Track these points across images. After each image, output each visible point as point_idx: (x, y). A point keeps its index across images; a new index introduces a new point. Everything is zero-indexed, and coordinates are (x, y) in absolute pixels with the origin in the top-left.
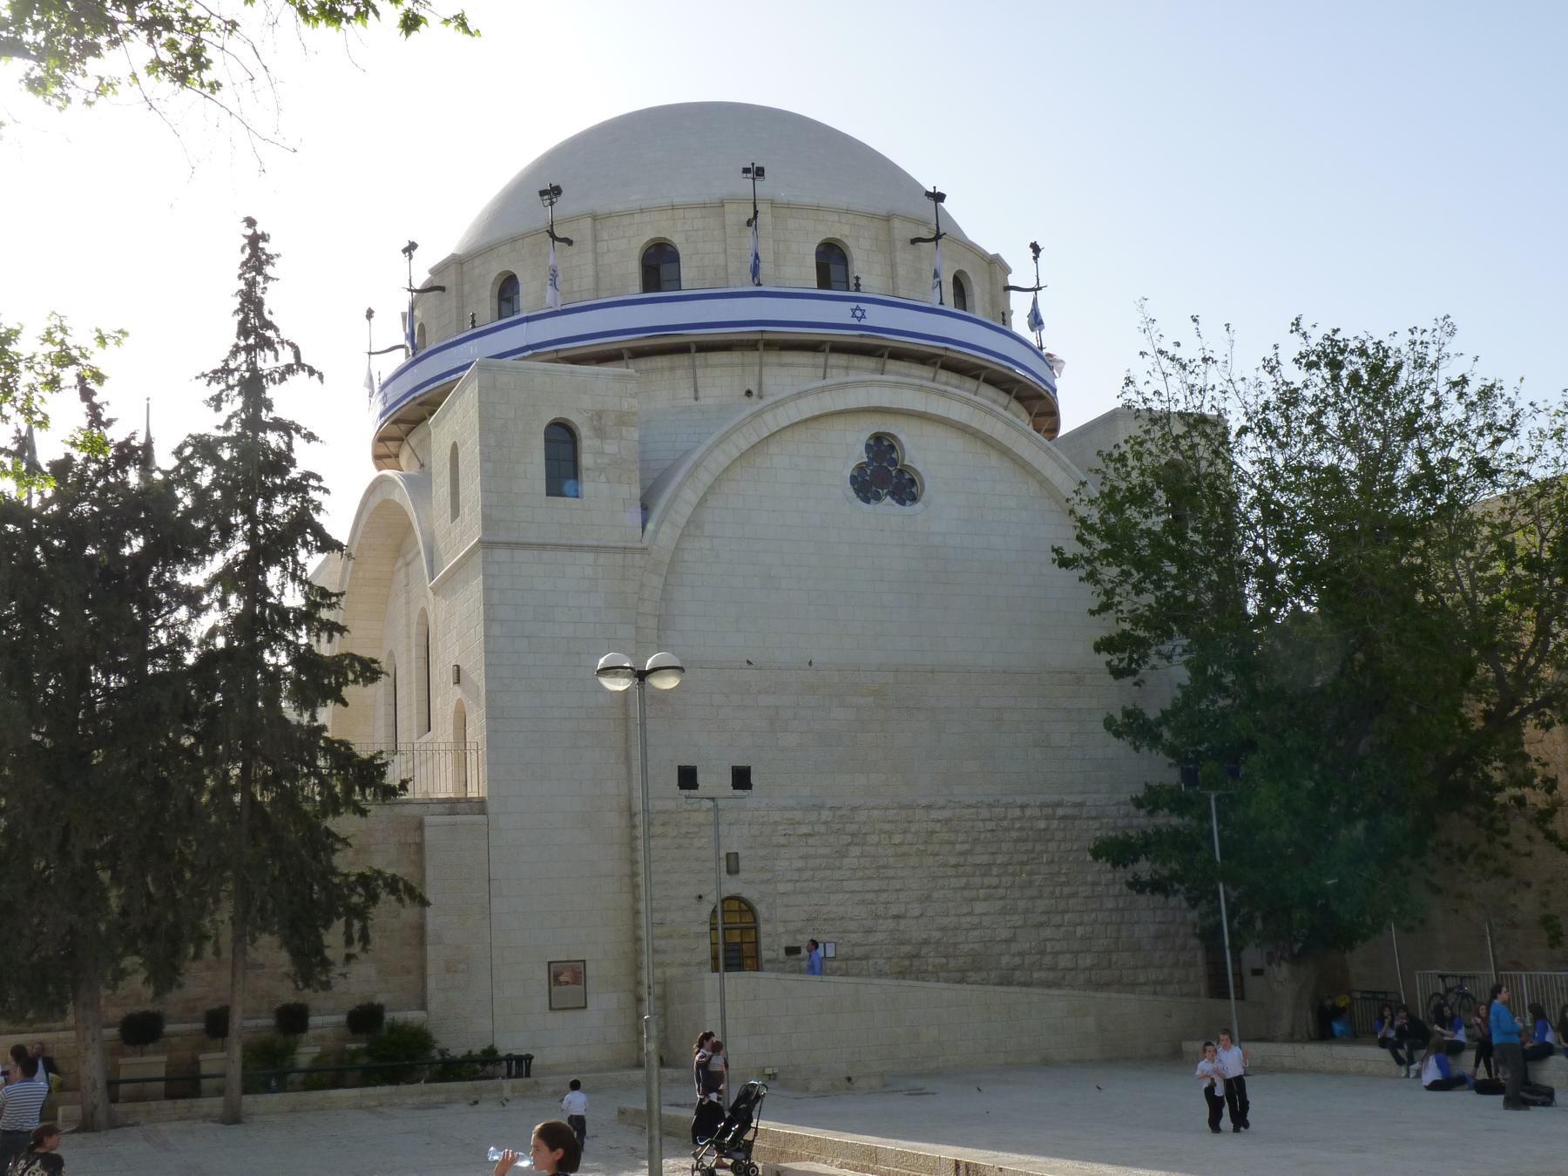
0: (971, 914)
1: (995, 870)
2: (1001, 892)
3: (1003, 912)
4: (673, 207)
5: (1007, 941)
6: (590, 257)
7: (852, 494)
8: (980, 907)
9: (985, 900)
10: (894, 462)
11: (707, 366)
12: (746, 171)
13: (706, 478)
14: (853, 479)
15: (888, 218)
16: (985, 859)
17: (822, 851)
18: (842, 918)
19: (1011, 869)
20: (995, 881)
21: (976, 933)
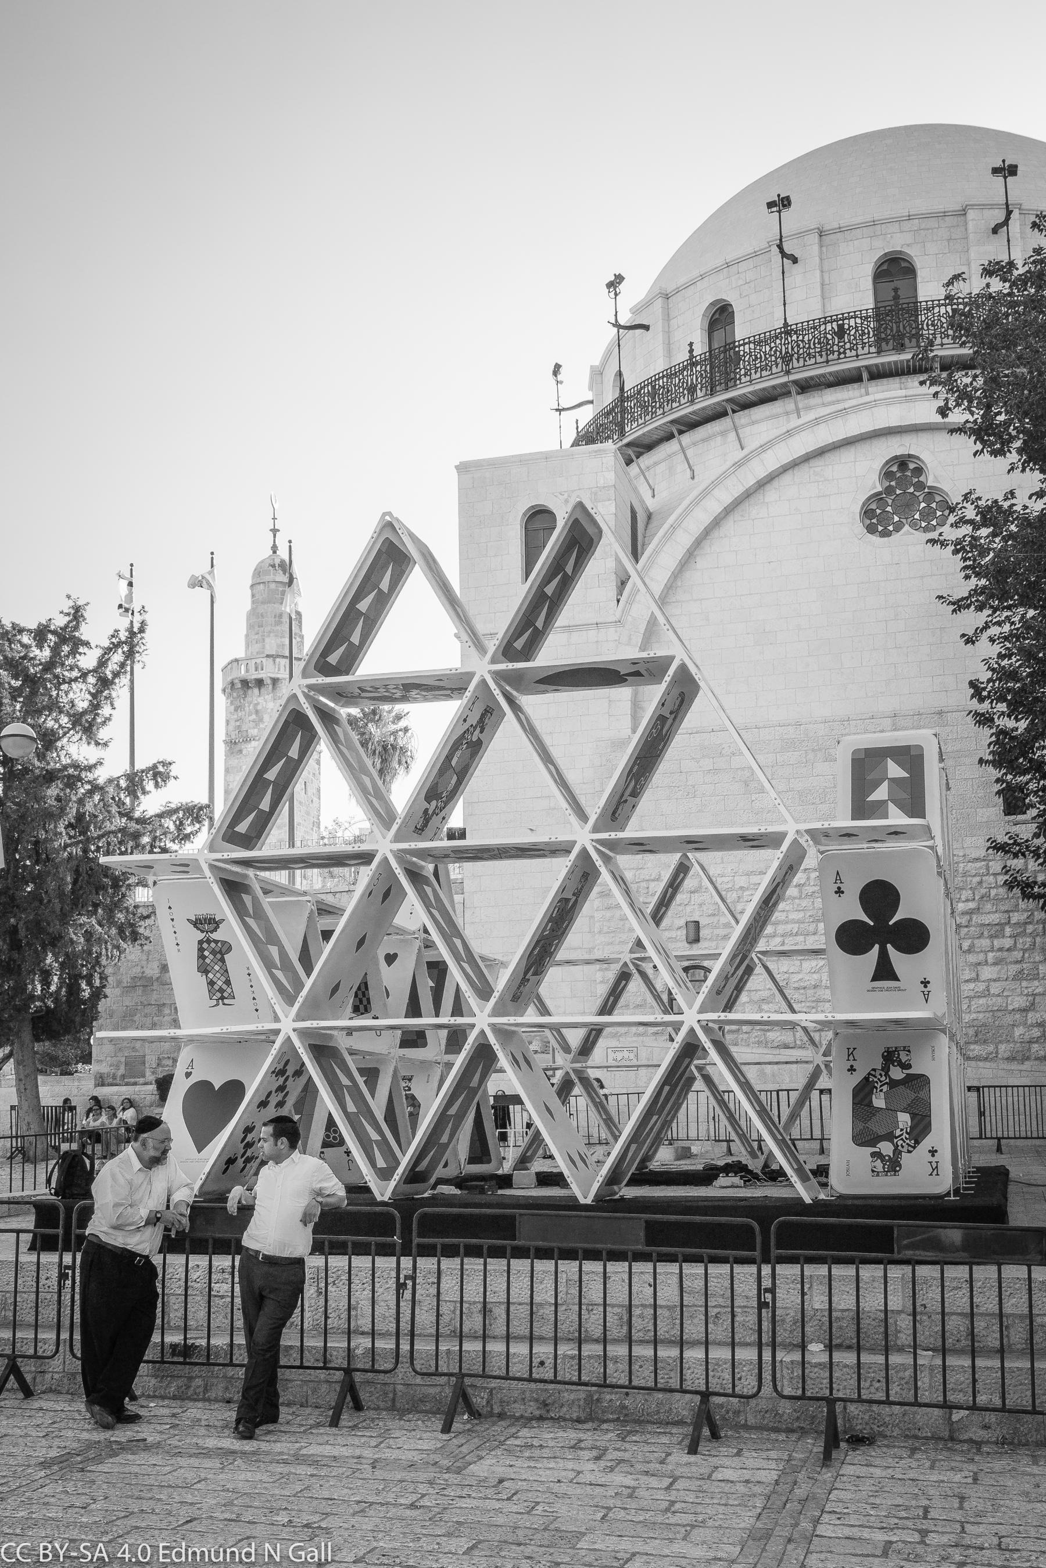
0: (977, 979)
1: (1008, 930)
2: (1017, 955)
3: (1019, 977)
4: (728, 265)
5: (1024, 1010)
6: (660, 337)
7: (860, 528)
8: (987, 973)
9: (995, 964)
10: (920, 486)
11: (753, 423)
12: (770, 205)
13: (684, 540)
14: (867, 513)
15: (963, 212)
16: (995, 918)
17: (793, 916)
18: (815, 987)
19: (1030, 928)
20: (1008, 943)
21: (982, 1001)
